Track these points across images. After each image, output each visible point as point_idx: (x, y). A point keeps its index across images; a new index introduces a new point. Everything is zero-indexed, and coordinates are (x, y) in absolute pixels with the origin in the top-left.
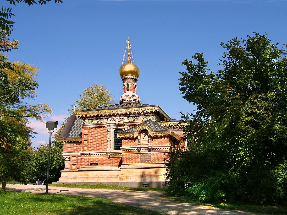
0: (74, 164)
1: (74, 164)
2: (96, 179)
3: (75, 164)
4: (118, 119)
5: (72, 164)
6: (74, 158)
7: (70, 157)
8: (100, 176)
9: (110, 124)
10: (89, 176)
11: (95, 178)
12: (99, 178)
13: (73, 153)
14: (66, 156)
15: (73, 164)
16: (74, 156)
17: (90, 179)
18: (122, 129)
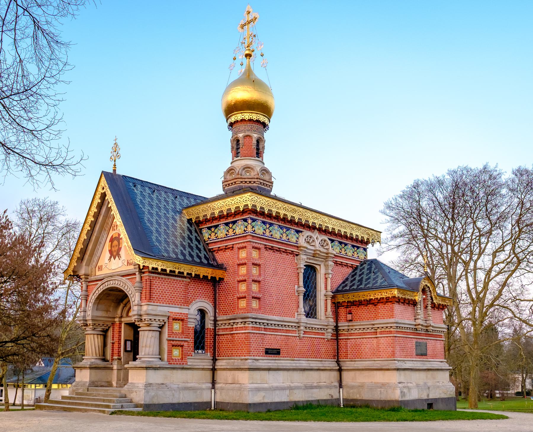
0: (179, 346)
1: (179, 346)
2: (287, 392)
3: (182, 343)
4: (319, 240)
5: (173, 346)
6: (177, 326)
7: (165, 323)
8: (292, 385)
9: (307, 248)
10: (271, 385)
11: (283, 389)
12: (291, 388)
13: (176, 310)
14: (157, 318)
15: (176, 346)
16: (176, 320)
17: (277, 392)
18: (316, 266)
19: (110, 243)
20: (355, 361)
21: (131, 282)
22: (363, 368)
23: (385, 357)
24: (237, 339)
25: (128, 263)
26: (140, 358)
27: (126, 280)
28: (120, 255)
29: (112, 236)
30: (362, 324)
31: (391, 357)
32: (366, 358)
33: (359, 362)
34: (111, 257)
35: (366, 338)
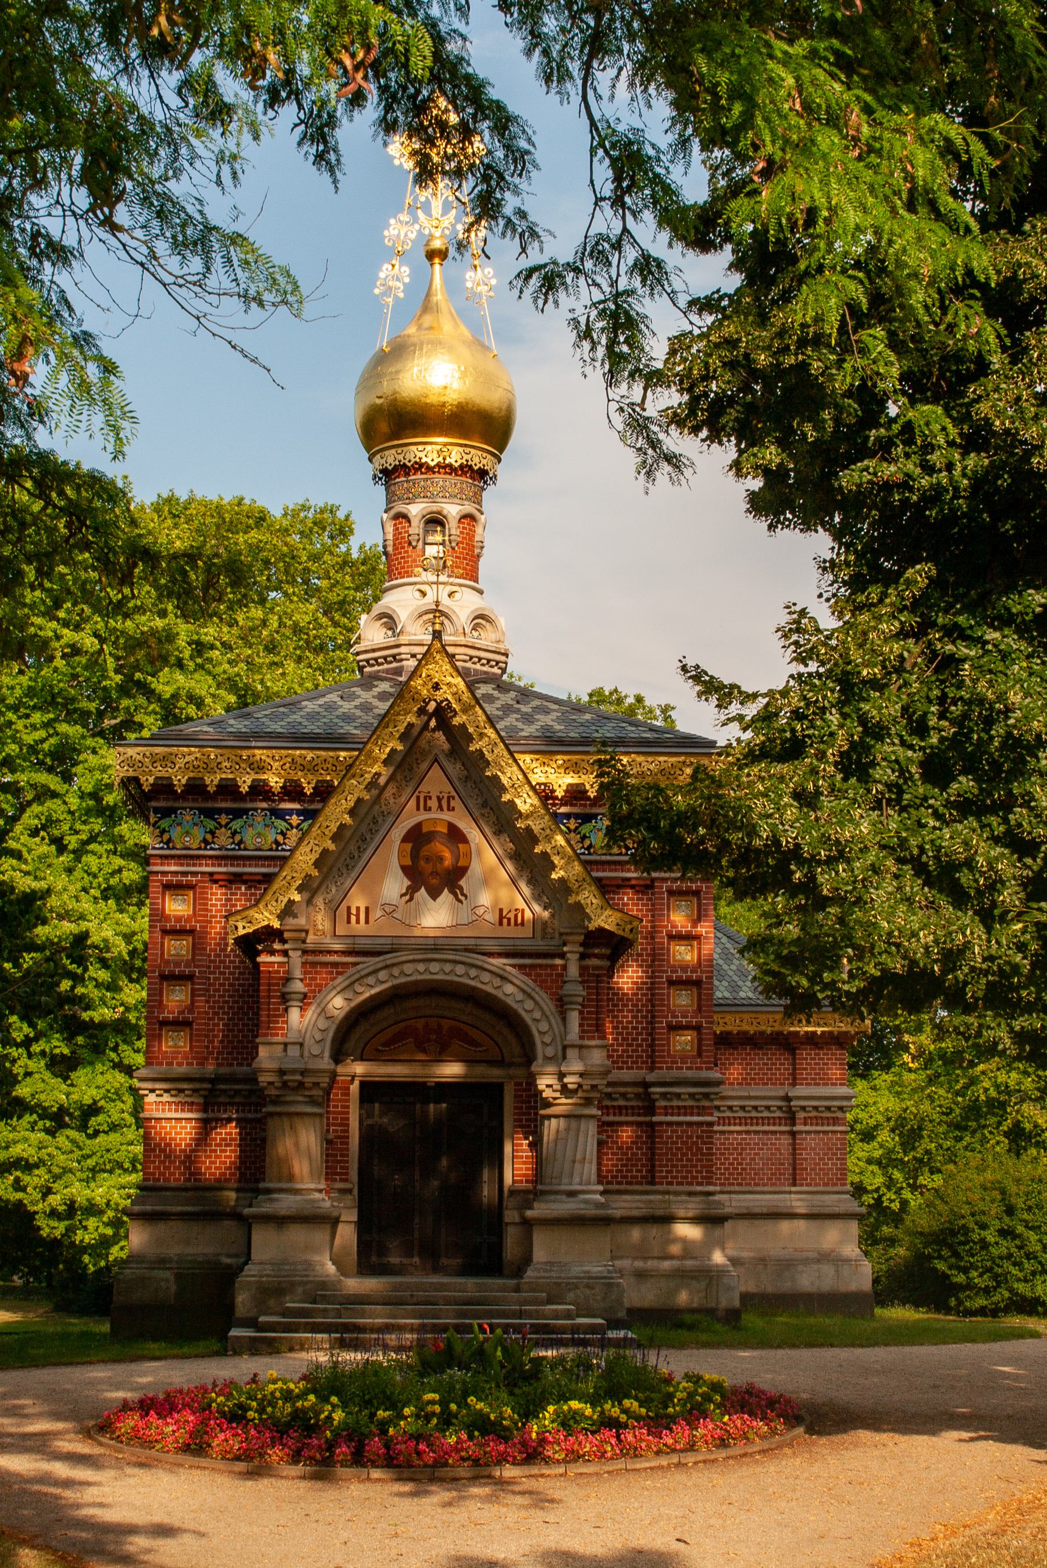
19: (409, 846)
20: (730, 1192)
21: (528, 975)
22: (765, 1211)
23: (817, 1185)
24: (671, 1137)
25: (501, 918)
26: (572, 1194)
27: (508, 968)
28: (461, 889)
29: (419, 826)
30: (752, 1094)
31: (835, 1185)
32: (756, 1185)
33: (741, 1196)
34: (411, 891)
35: (756, 1132)
